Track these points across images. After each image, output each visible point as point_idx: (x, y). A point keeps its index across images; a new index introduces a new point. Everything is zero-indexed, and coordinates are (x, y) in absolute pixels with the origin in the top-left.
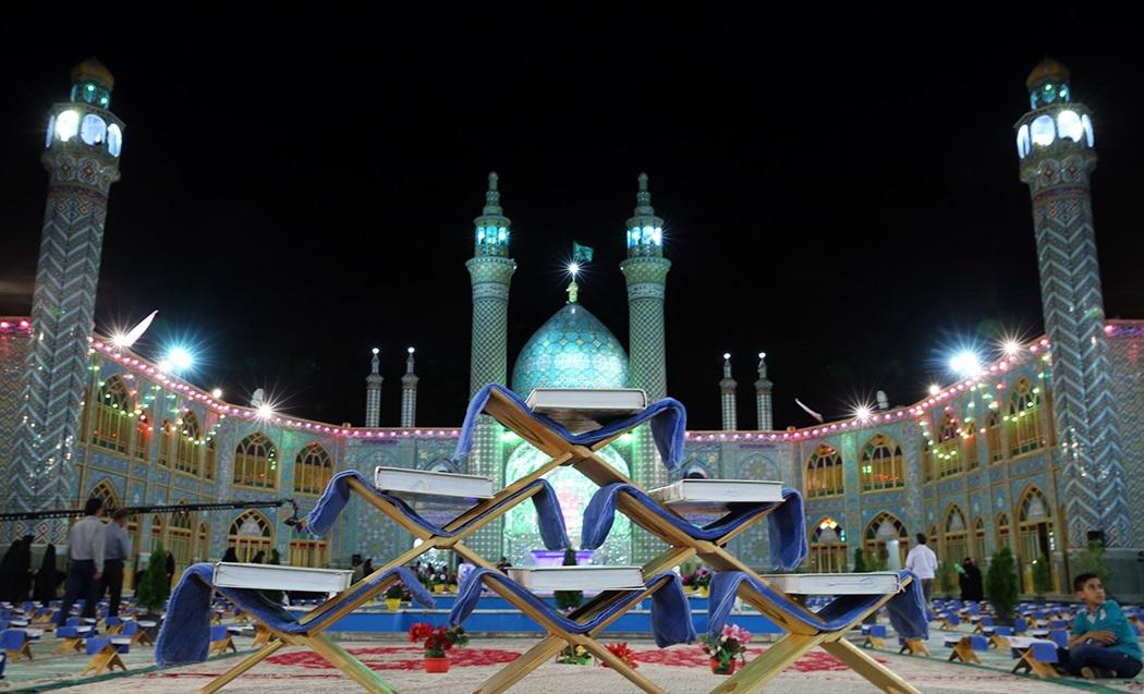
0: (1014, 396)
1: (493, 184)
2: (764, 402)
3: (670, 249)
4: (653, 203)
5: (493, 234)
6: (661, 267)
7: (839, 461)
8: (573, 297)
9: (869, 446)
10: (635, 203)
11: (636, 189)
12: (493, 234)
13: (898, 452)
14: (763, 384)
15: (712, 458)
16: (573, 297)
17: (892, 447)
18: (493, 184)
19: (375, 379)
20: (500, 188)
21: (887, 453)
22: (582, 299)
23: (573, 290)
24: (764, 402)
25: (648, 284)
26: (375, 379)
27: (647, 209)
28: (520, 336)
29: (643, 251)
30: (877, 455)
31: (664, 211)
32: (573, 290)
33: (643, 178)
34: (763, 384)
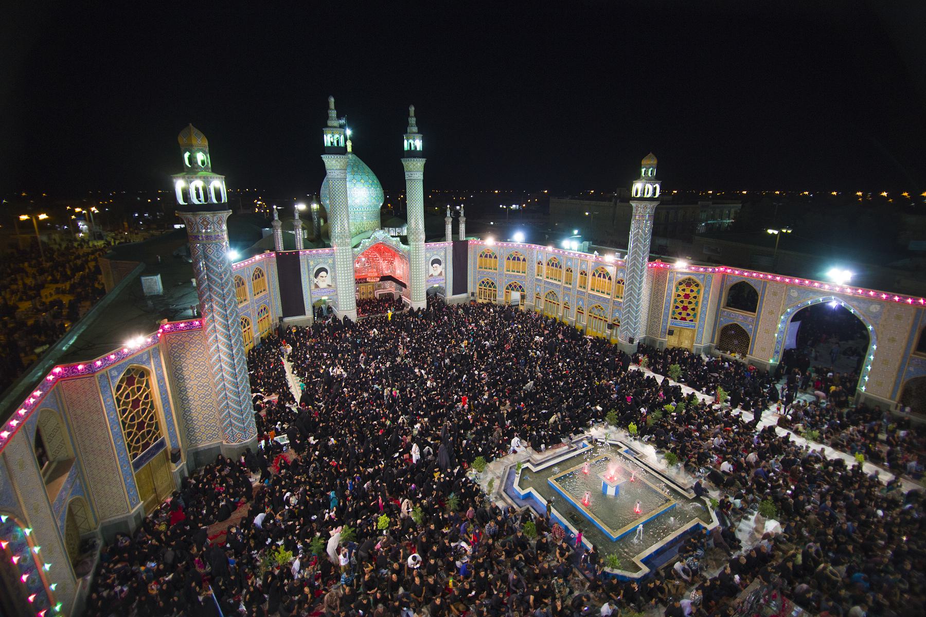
0: (597, 271)
1: (332, 105)
2: (462, 227)
7: (496, 257)
9: (511, 255)
11: (408, 115)
13: (524, 260)
14: (462, 220)
15: (442, 254)
17: (522, 258)
18: (332, 105)
21: (519, 259)
24: (462, 227)
25: (415, 171)
27: (415, 129)
29: (413, 154)
30: (514, 259)
33: (412, 109)
34: (462, 220)
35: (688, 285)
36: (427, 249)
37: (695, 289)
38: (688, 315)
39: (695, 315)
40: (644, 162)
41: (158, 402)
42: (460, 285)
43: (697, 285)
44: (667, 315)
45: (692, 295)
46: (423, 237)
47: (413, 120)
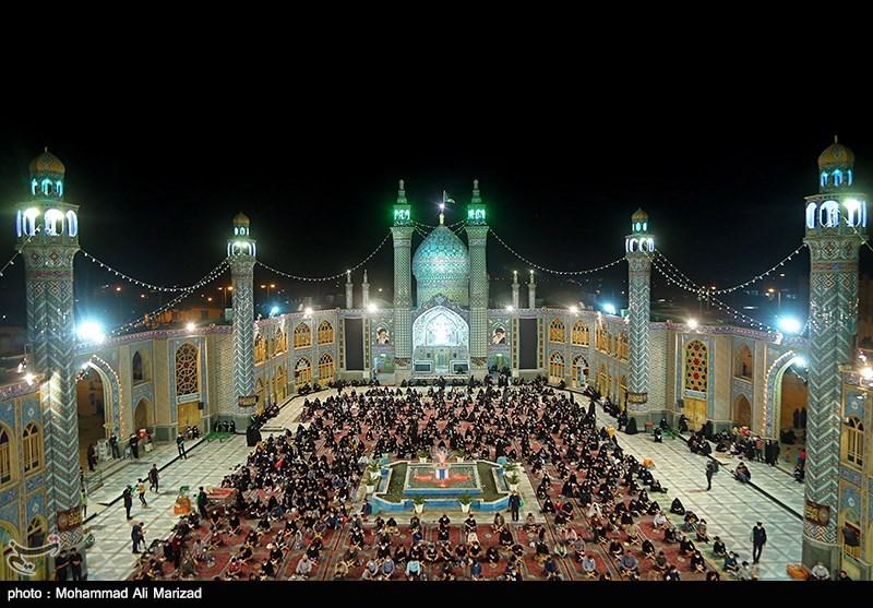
1: (402, 187)
3: (489, 221)
4: (481, 196)
5: (402, 213)
6: (483, 231)
8: (442, 222)
10: (471, 195)
12: (402, 213)
16: (442, 222)
19: (349, 286)
20: (405, 189)
22: (446, 224)
23: (442, 217)
24: (532, 294)
26: (349, 286)
27: (478, 200)
28: (416, 243)
31: (486, 199)
32: (442, 217)
33: (476, 182)
34: (532, 286)
35: (697, 348)
36: (489, 317)
37: (703, 353)
38: (700, 384)
39: (705, 384)
40: (634, 217)
41: (199, 370)
42: (528, 360)
43: (704, 349)
44: (679, 383)
45: (702, 359)
46: (485, 302)
47: (476, 192)
